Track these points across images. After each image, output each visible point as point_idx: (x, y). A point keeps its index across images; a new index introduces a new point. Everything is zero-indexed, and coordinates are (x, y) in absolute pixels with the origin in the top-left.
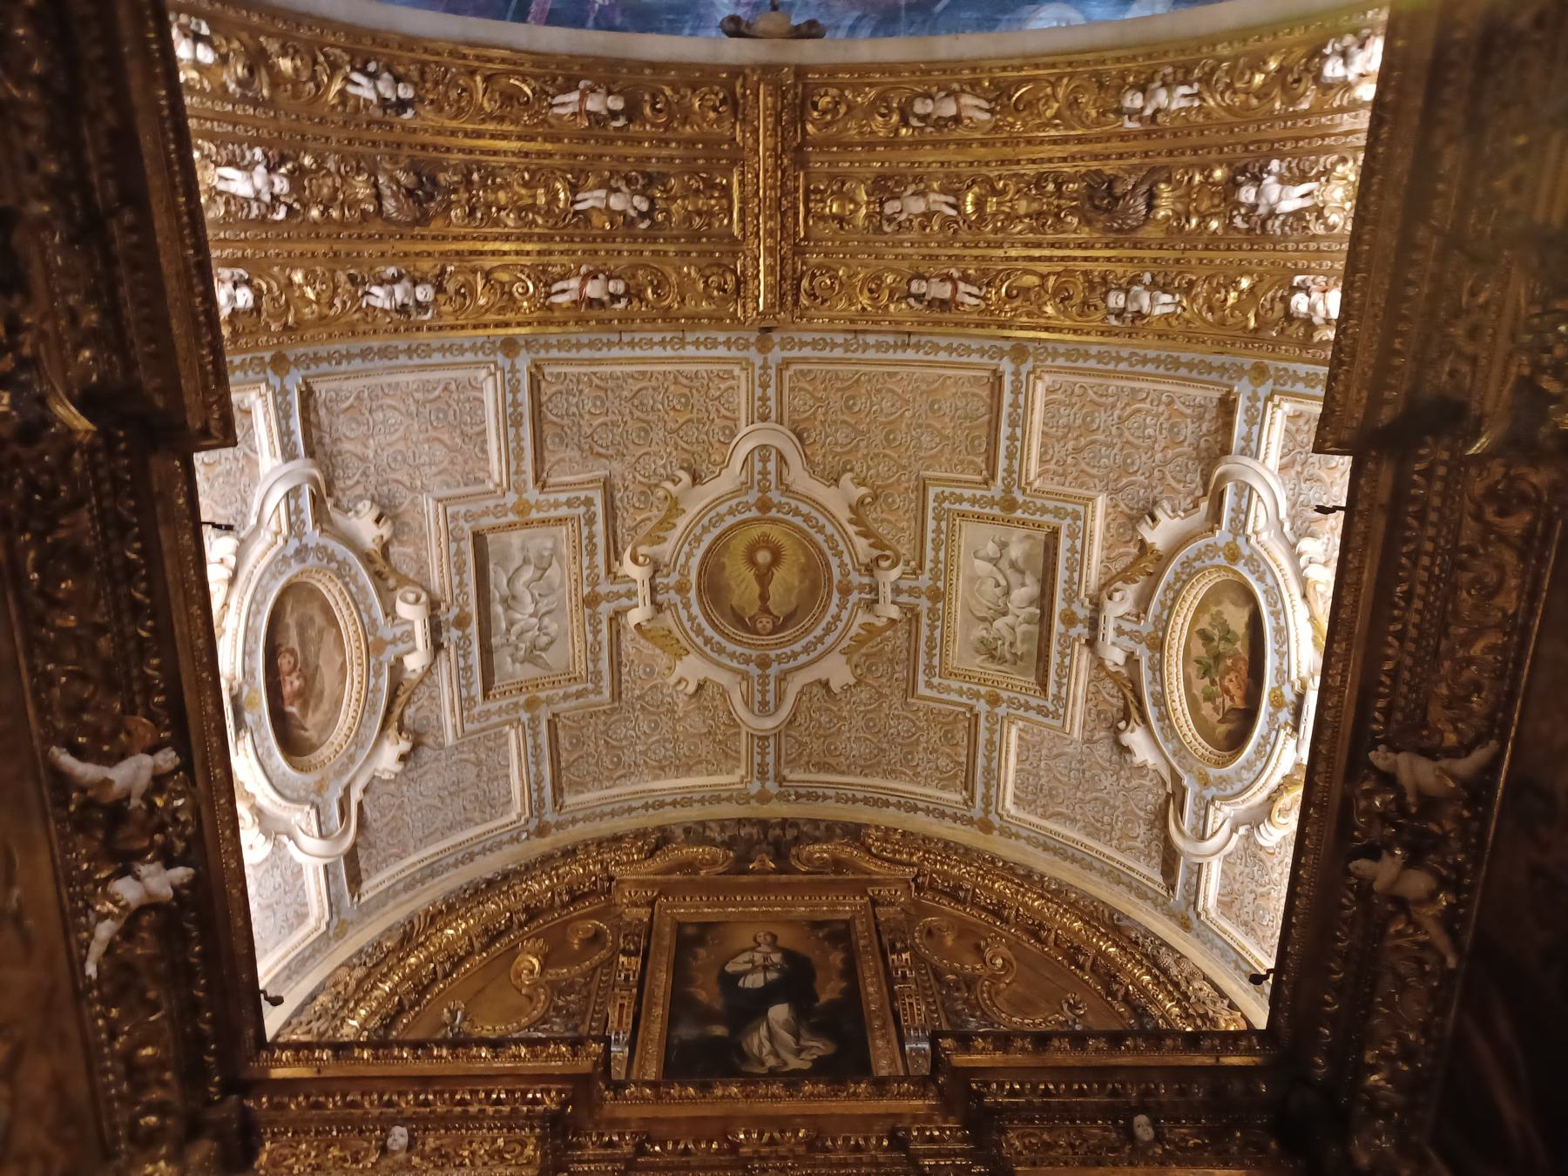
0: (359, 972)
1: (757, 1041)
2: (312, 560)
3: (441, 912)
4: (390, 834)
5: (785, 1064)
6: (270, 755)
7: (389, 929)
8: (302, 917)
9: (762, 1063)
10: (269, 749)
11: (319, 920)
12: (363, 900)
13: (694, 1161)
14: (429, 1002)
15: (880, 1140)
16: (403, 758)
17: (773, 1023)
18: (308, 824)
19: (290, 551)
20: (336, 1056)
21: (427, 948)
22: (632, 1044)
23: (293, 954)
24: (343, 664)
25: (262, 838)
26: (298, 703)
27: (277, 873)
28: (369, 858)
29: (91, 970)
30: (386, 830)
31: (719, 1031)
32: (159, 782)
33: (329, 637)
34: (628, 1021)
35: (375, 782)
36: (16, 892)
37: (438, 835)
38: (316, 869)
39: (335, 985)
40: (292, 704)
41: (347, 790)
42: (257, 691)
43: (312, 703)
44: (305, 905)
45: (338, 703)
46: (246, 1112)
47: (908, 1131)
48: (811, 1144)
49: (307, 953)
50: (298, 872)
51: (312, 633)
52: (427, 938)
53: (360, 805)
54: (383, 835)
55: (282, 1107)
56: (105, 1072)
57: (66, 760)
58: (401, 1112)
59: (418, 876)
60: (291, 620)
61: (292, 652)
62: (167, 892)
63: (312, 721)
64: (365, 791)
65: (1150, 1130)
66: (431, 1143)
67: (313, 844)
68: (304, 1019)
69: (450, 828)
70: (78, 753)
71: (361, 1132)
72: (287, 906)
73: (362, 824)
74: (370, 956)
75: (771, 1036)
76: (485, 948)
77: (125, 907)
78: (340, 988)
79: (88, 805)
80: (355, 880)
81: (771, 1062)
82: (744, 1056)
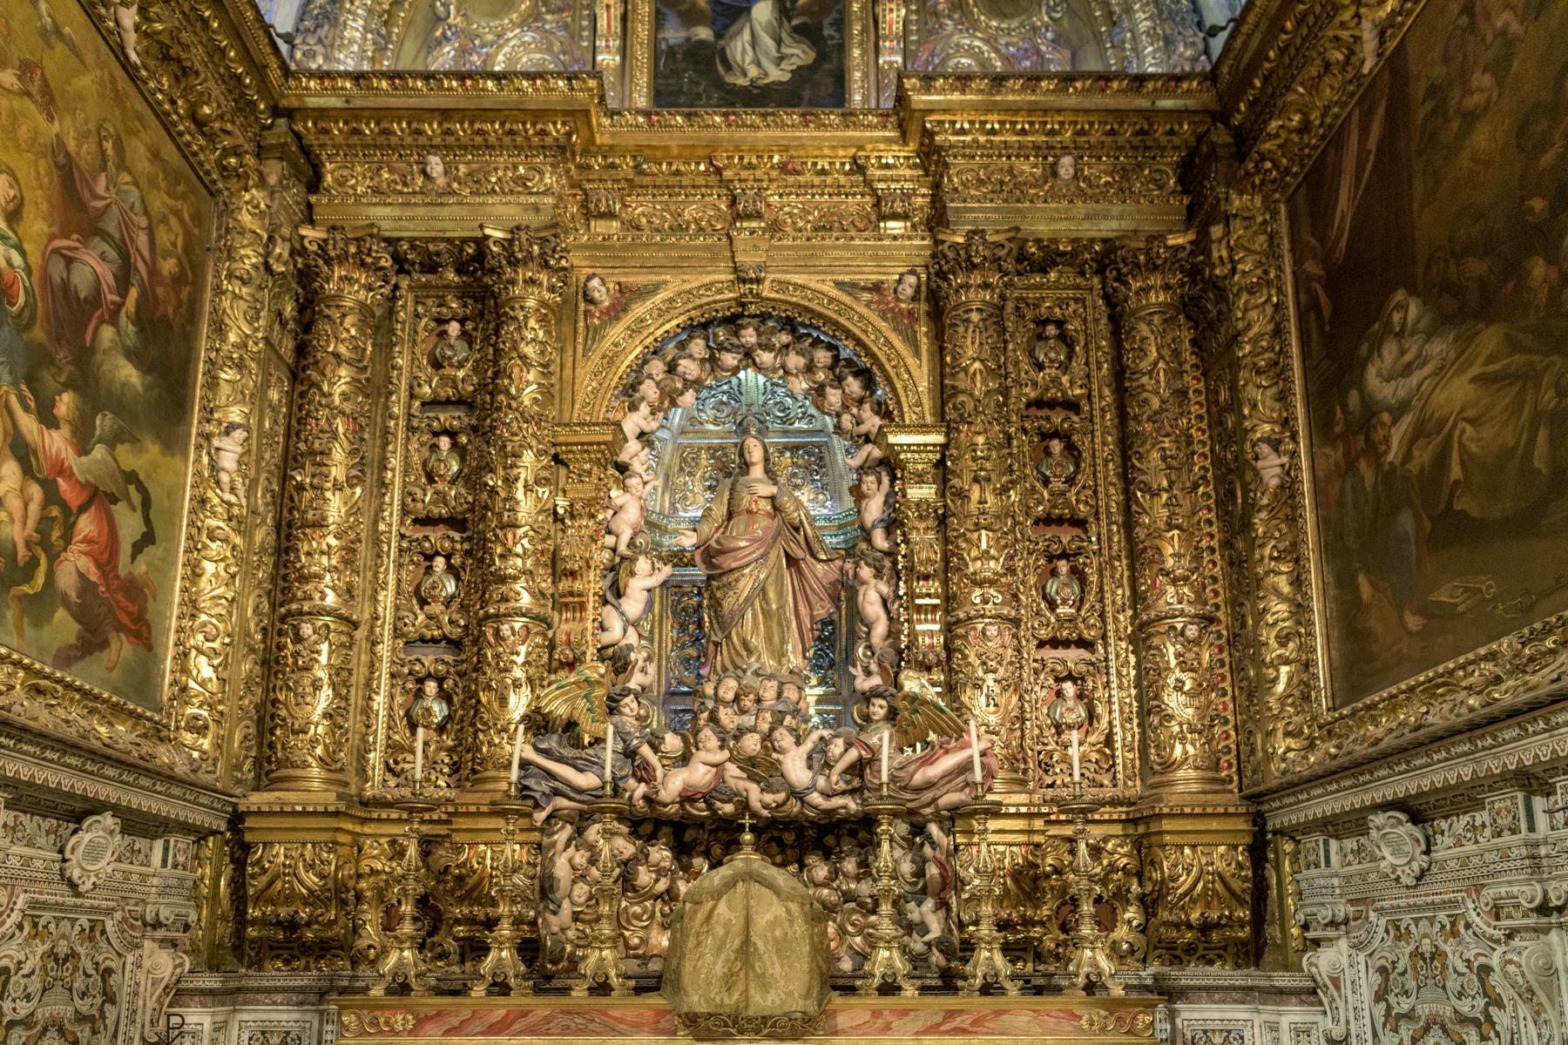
1: (739, 48)
5: (766, 74)
9: (745, 74)
13: (686, 181)
15: (843, 164)
17: (757, 27)
22: (624, 51)
31: (704, 33)
34: (616, 26)
47: (868, 157)
48: (783, 168)
65: (1071, 171)
66: (463, 169)
75: (754, 42)
81: (753, 72)
82: (728, 67)
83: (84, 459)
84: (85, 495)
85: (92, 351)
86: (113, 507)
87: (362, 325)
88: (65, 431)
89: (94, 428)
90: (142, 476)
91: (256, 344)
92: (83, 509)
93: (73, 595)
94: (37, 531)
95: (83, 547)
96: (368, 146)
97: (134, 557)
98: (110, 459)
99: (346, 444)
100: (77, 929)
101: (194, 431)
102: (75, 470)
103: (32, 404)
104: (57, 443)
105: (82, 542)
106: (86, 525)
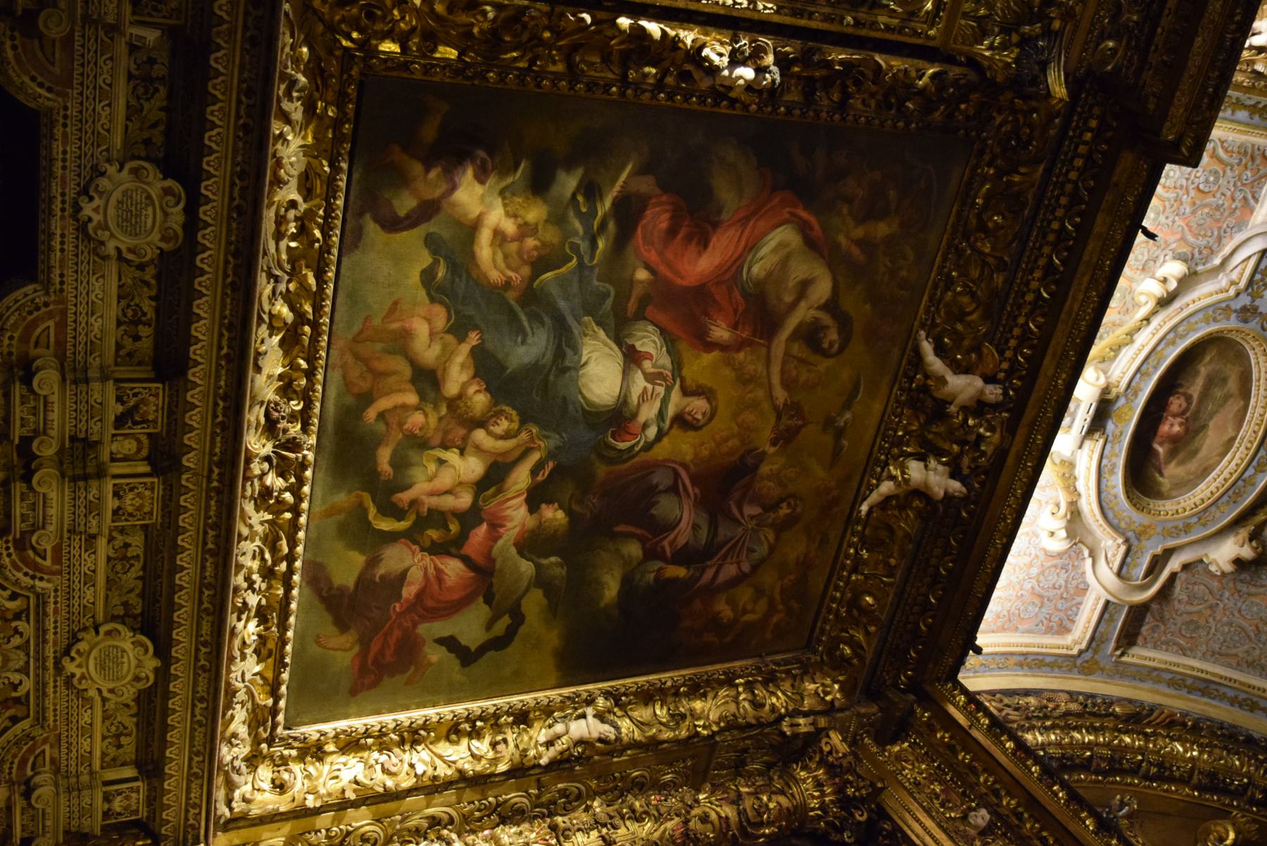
0: (1074, 707)
2: (1254, 324)
3: (1185, 725)
4: (1187, 624)
6: (1112, 472)
7: (1130, 701)
8: (1063, 629)
10: (1114, 466)
11: (1076, 643)
12: (1125, 659)
14: (1115, 782)
16: (1238, 562)
18: (1114, 556)
19: (1237, 305)
20: (990, 727)
21: (1147, 741)
23: (1036, 650)
24: (1233, 439)
25: (1063, 534)
26: (1167, 445)
27: (1063, 575)
28: (1153, 629)
29: (864, 508)
30: (1186, 618)
32: (979, 407)
33: (1233, 407)
35: (1200, 567)
36: (848, 416)
37: (1234, 662)
38: (1098, 599)
39: (1049, 700)
40: (1161, 444)
41: (1168, 553)
42: (1132, 409)
43: (1181, 455)
44: (1073, 622)
45: (1205, 472)
46: (912, 712)
49: (1048, 660)
50: (1083, 590)
51: (1218, 393)
52: (1154, 734)
53: (1173, 576)
54: (1179, 620)
55: (934, 731)
56: (837, 588)
57: (927, 347)
58: (999, 805)
59: (1189, 682)
60: (1204, 369)
61: (1188, 398)
62: (939, 493)
63: (1172, 471)
64: (1186, 567)
67: (1107, 574)
68: (1006, 701)
69: (1251, 665)
70: (940, 351)
71: (964, 794)
72: (1056, 609)
73: (1165, 593)
74: (1094, 705)
76: (1202, 788)
77: (906, 481)
78: (1051, 705)
79: (925, 389)
80: (1129, 637)
83: (513, 551)
84: (479, 560)
85: (615, 536)
86: (481, 599)
87: (784, 813)
88: (531, 522)
89: (547, 557)
90: (523, 629)
91: (704, 727)
92: (466, 560)
93: (381, 571)
94: (429, 510)
95: (431, 571)
96: (951, 766)
97: (441, 641)
98: (524, 583)
99: (657, 835)
100: (16, 678)
101: (590, 687)
102: (500, 543)
103: (540, 478)
104: (517, 515)
105: (436, 568)
106: (453, 568)
